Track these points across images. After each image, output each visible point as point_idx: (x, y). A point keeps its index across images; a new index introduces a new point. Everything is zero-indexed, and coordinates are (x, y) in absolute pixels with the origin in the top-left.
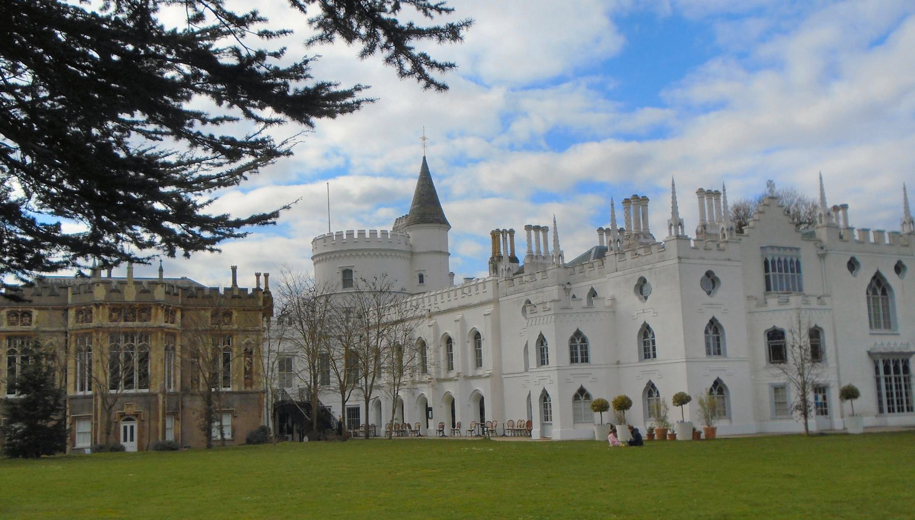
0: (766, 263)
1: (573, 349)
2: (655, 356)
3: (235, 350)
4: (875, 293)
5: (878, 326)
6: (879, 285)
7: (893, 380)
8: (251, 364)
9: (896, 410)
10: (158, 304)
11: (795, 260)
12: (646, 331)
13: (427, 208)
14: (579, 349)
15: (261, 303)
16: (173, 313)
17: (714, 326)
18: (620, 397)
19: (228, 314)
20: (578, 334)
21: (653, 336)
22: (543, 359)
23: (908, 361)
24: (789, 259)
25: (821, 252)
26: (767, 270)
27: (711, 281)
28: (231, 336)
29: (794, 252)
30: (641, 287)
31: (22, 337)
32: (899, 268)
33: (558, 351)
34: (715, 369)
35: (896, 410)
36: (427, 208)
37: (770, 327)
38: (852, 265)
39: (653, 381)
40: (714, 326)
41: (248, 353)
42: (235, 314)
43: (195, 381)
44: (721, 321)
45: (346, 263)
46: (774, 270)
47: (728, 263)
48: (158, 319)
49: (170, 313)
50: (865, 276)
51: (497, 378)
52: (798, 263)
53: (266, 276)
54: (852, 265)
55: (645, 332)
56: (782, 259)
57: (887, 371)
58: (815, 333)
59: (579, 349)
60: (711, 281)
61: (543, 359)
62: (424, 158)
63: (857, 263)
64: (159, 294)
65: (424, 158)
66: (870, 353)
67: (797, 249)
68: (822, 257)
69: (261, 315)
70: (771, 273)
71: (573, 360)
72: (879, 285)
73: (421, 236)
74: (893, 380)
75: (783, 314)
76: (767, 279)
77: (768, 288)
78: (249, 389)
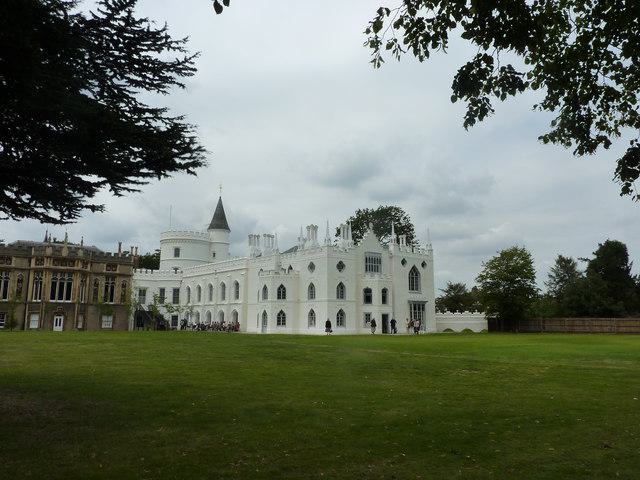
1: (279, 292)
6: (414, 272)
10: (78, 259)
12: (312, 287)
13: (220, 221)
14: (282, 293)
16: (87, 264)
17: (341, 287)
19: (115, 266)
20: (282, 286)
22: (265, 296)
27: (341, 266)
30: (312, 267)
31: (62, 272)
32: (423, 265)
33: (272, 293)
36: (220, 221)
40: (341, 287)
41: (124, 286)
43: (95, 298)
45: (177, 245)
48: (79, 266)
49: (85, 264)
50: (408, 267)
51: (245, 306)
54: (404, 262)
57: (415, 309)
58: (384, 291)
59: (282, 293)
60: (341, 266)
61: (265, 296)
62: (220, 200)
64: (81, 253)
65: (220, 200)
66: (409, 302)
68: (391, 258)
71: (279, 298)
72: (414, 272)
73: (216, 236)
75: (374, 282)
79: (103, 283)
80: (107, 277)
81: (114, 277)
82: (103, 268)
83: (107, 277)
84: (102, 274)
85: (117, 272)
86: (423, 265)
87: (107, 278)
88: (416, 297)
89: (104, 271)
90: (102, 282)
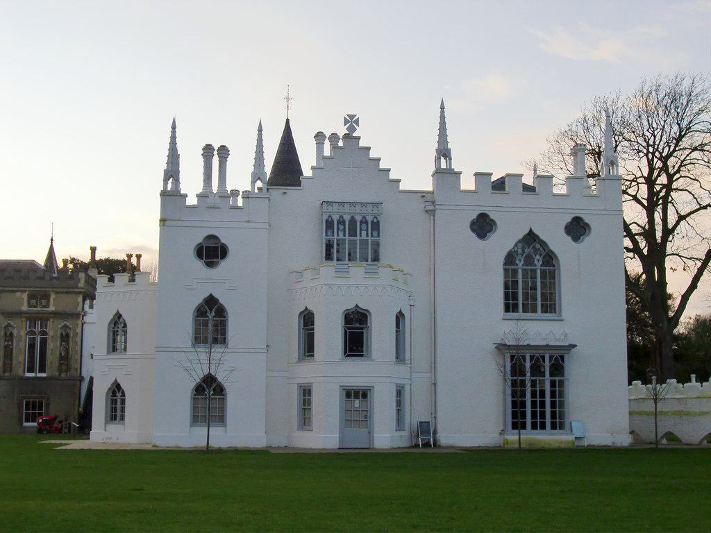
3: (51, 333)
4: (529, 260)
5: (530, 308)
7: (528, 384)
8: (67, 350)
9: (529, 425)
11: (370, 219)
15: (82, 284)
19: (47, 297)
23: (562, 358)
24: (358, 218)
28: (47, 319)
34: (198, 363)
35: (529, 425)
41: (65, 338)
42: (53, 297)
44: (223, 300)
50: (505, 238)
52: (376, 226)
53: (139, 257)
56: (347, 218)
62: (288, 121)
65: (288, 121)
69: (80, 299)
74: (528, 384)
78: (63, 375)
79: (23, 333)
80: (32, 318)
81: (44, 318)
82: (21, 301)
83: (32, 318)
84: (19, 314)
85: (52, 308)
87: (33, 325)
88: (536, 331)
89: (25, 308)
90: (21, 331)
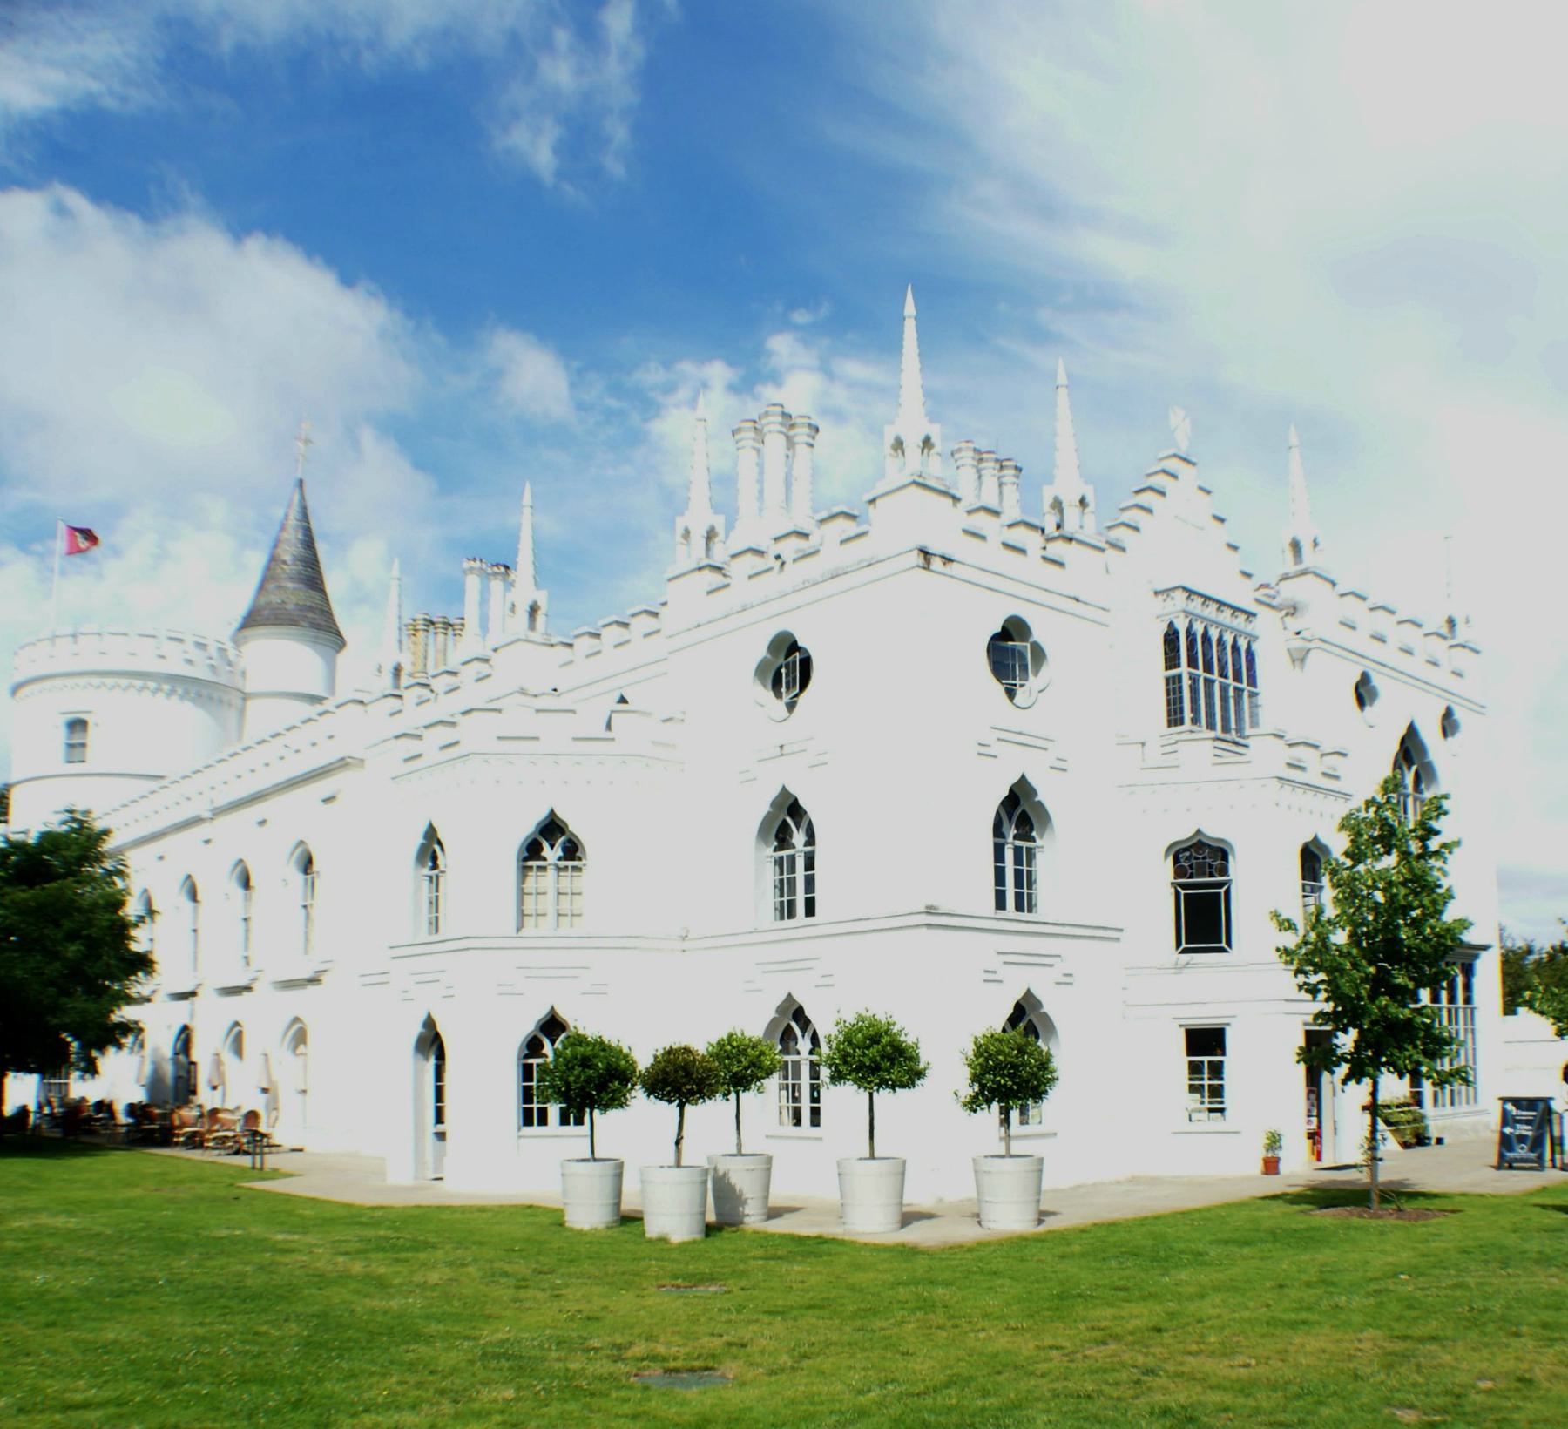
0: (1171, 639)
2: (810, 909)
18: (670, 1051)
21: (811, 839)
25: (1297, 643)
26: (1171, 660)
29: (1239, 622)
32: (1449, 724)
37: (1184, 833)
38: (1364, 693)
39: (800, 999)
45: (77, 700)
46: (1192, 663)
47: (1071, 606)
54: (1364, 693)
55: (784, 828)
63: (1373, 695)
67: (1250, 615)
70: (1184, 669)
76: (1173, 685)
77: (1175, 718)
86: (1449, 724)
